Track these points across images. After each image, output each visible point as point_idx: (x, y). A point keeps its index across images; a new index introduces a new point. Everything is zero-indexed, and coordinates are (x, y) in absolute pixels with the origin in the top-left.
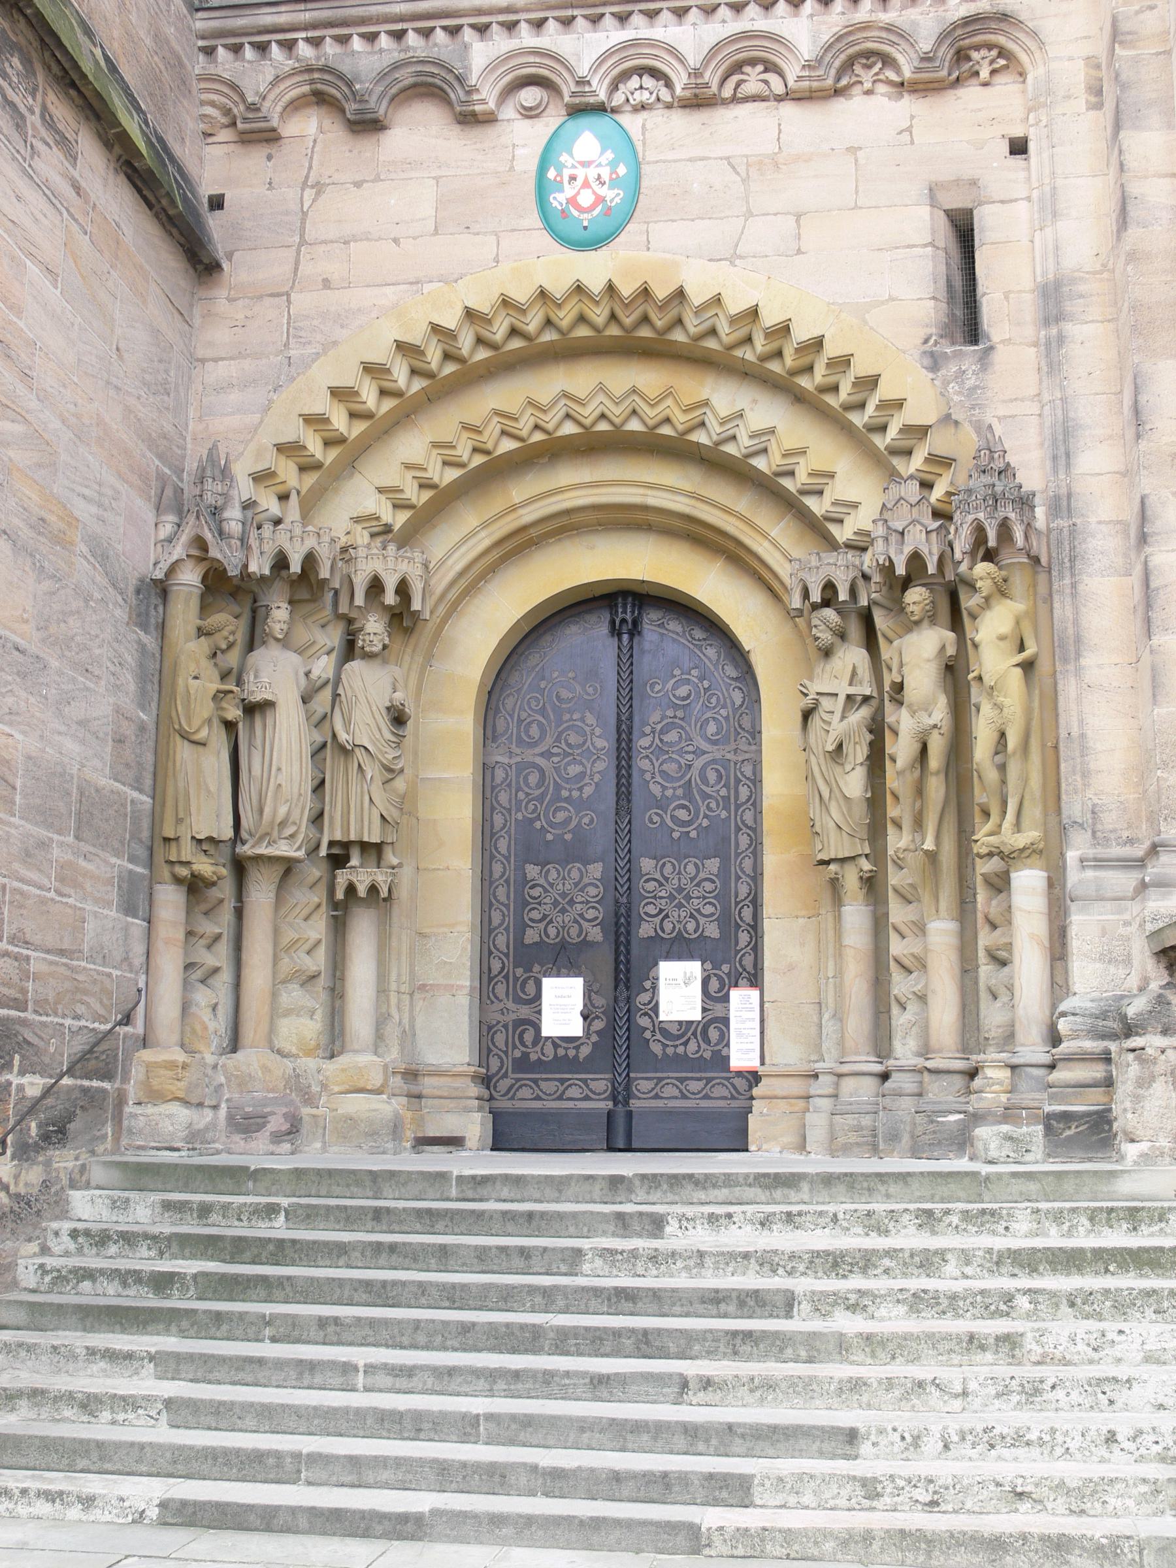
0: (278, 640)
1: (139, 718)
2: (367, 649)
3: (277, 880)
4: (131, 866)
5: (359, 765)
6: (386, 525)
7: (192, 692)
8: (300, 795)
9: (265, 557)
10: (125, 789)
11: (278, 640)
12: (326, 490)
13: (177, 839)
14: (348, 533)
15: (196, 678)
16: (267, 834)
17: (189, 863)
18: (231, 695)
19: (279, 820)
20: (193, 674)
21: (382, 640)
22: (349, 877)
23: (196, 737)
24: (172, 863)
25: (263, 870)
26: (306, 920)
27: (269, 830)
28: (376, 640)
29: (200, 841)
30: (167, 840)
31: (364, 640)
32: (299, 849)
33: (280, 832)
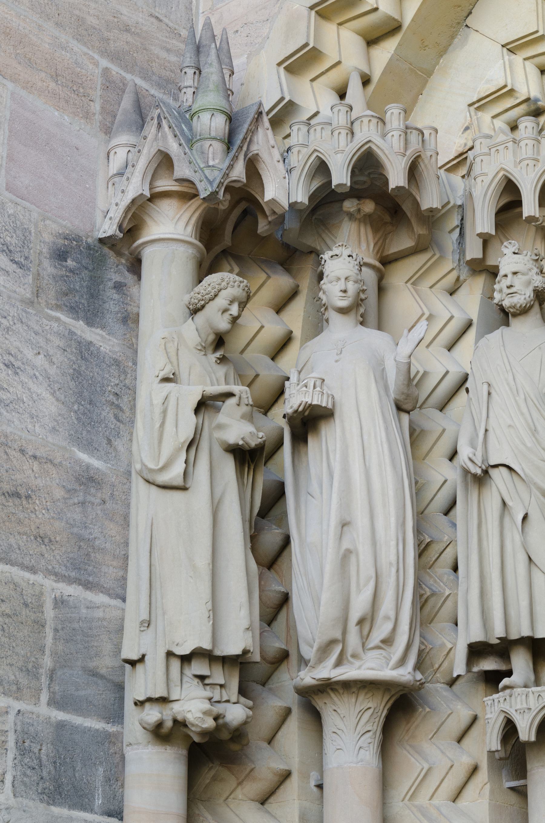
0: (343, 311)
1: (78, 462)
2: (506, 303)
3: (377, 726)
4: (61, 716)
5: (504, 503)
6: (528, 100)
7: (155, 402)
8: (391, 564)
9: (295, 174)
10: (39, 578)
11: (343, 311)
12: (429, 73)
13: (142, 659)
14: (467, 128)
15: (166, 380)
16: (332, 642)
17: (164, 700)
18: (232, 401)
19: (355, 615)
20: (162, 375)
21: (529, 283)
22: (505, 707)
23: (164, 478)
24: (139, 704)
25: (342, 710)
26: (456, 797)
27: (338, 635)
28: (518, 283)
29: (186, 659)
30: (133, 663)
31: (501, 291)
32: (402, 661)
33: (364, 639)
